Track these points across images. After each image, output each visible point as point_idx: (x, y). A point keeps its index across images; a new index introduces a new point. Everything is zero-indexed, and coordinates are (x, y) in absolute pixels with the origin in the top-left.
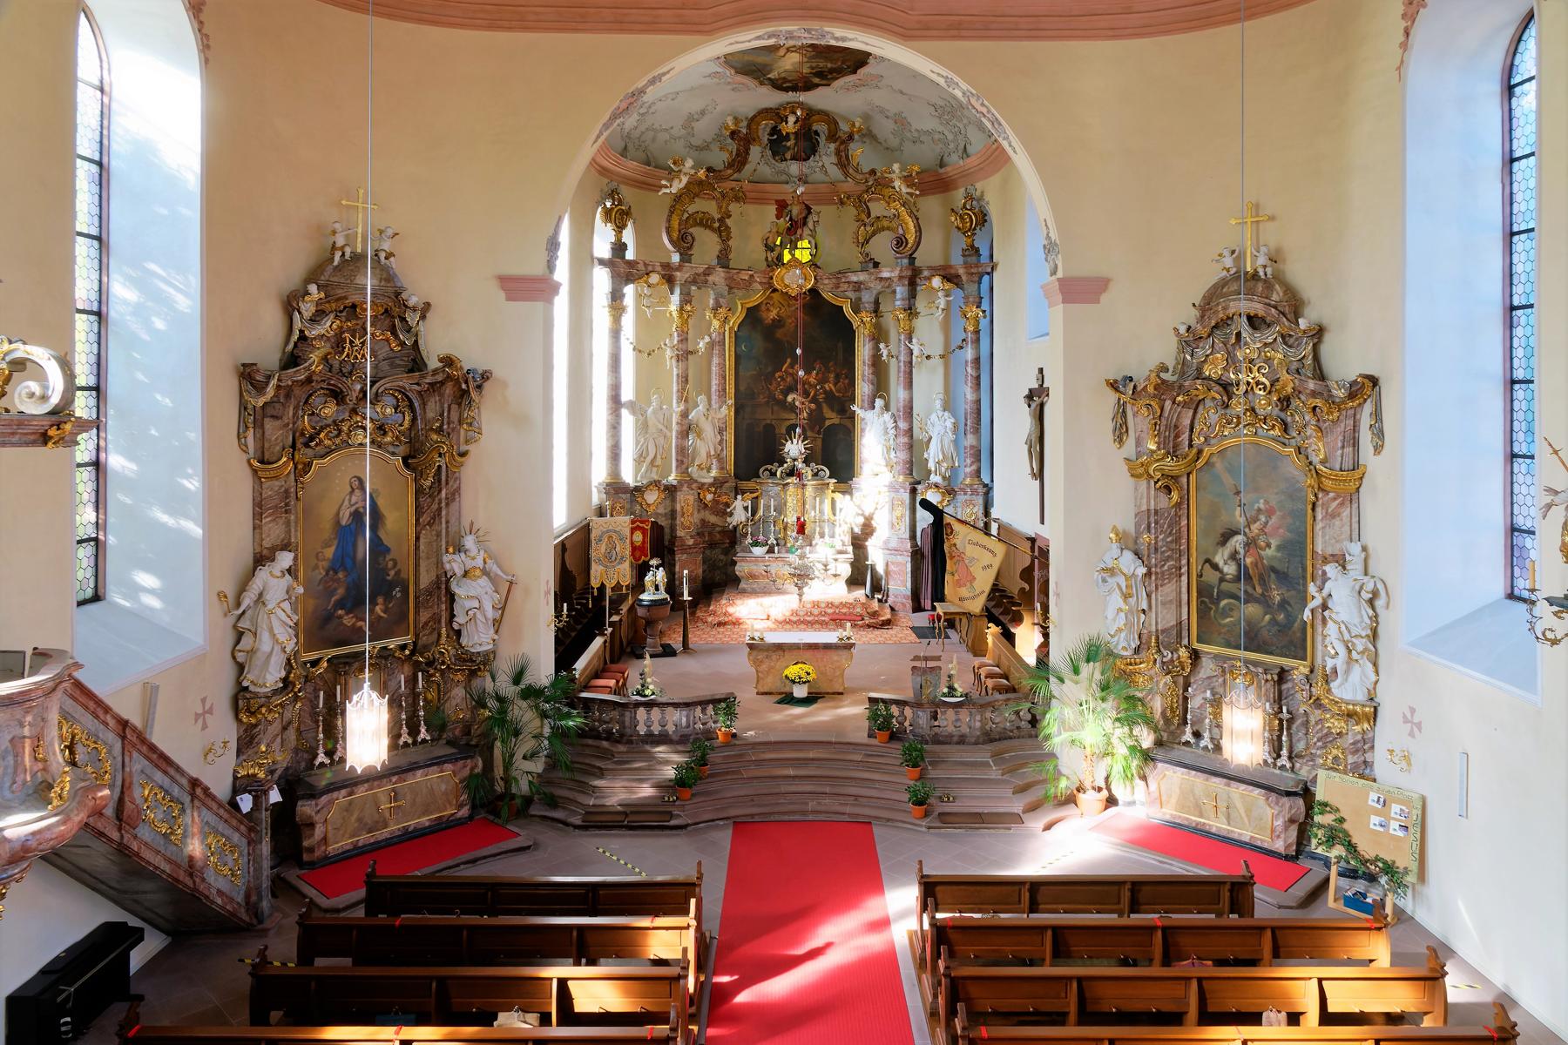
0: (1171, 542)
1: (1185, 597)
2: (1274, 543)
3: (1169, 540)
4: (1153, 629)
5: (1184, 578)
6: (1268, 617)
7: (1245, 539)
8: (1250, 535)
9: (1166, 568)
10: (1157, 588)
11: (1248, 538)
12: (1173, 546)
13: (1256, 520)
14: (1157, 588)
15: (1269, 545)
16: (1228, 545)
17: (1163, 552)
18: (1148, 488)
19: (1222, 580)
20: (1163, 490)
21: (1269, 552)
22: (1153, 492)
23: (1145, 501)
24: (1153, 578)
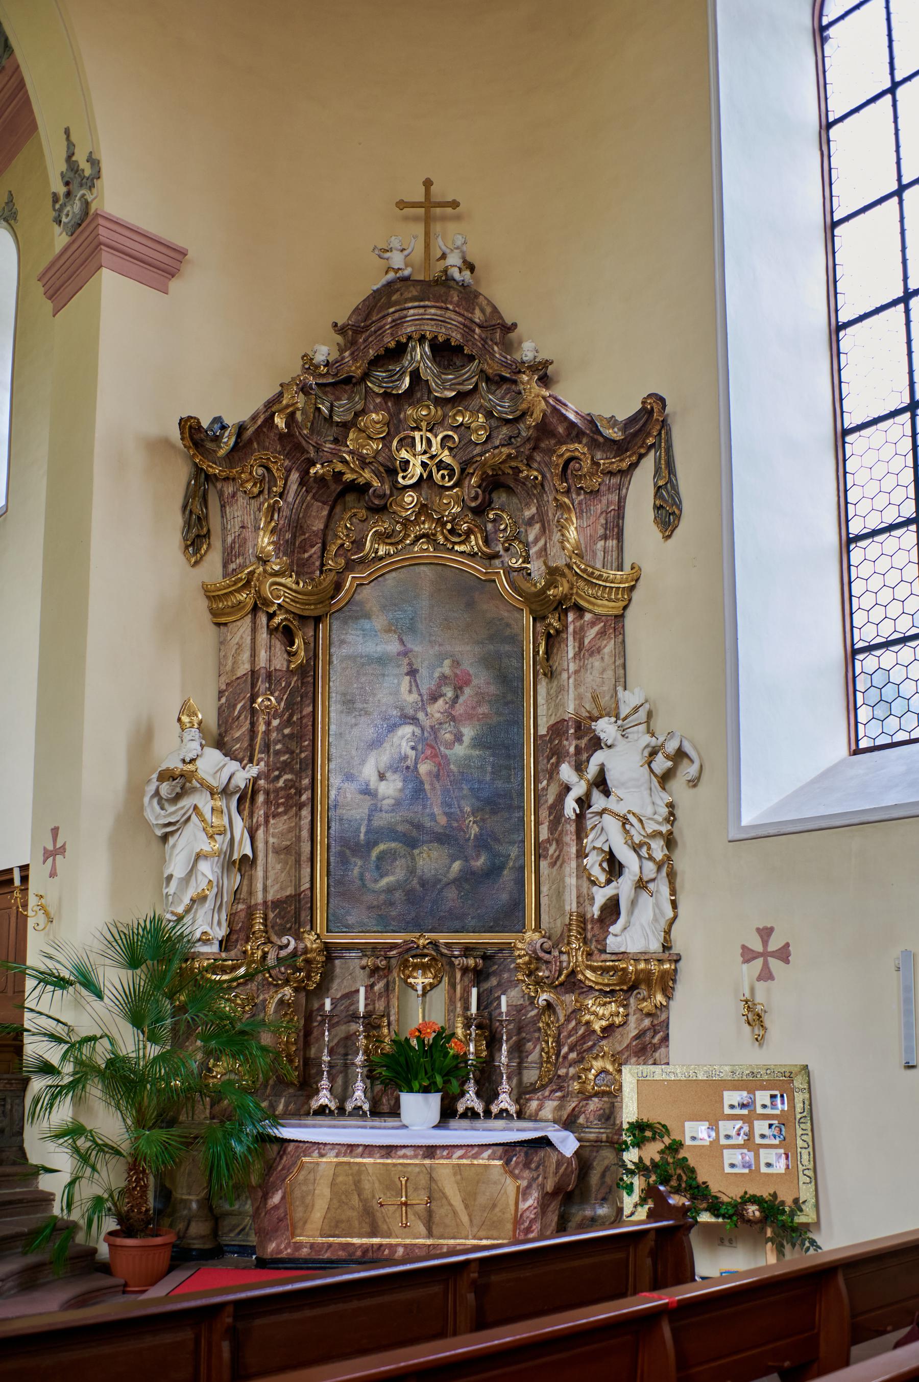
0: (291, 736)
1: (306, 848)
2: (468, 732)
3: (287, 731)
4: (259, 897)
5: (306, 812)
6: (457, 866)
7: (418, 731)
8: (427, 723)
9: (281, 783)
10: (267, 822)
11: (423, 730)
12: (293, 745)
13: (434, 698)
14: (267, 822)
15: (458, 738)
16: (386, 745)
17: (278, 753)
18: (254, 630)
19: (375, 809)
20: (279, 635)
21: (460, 750)
22: (263, 635)
23: (246, 655)
24: (261, 798)
